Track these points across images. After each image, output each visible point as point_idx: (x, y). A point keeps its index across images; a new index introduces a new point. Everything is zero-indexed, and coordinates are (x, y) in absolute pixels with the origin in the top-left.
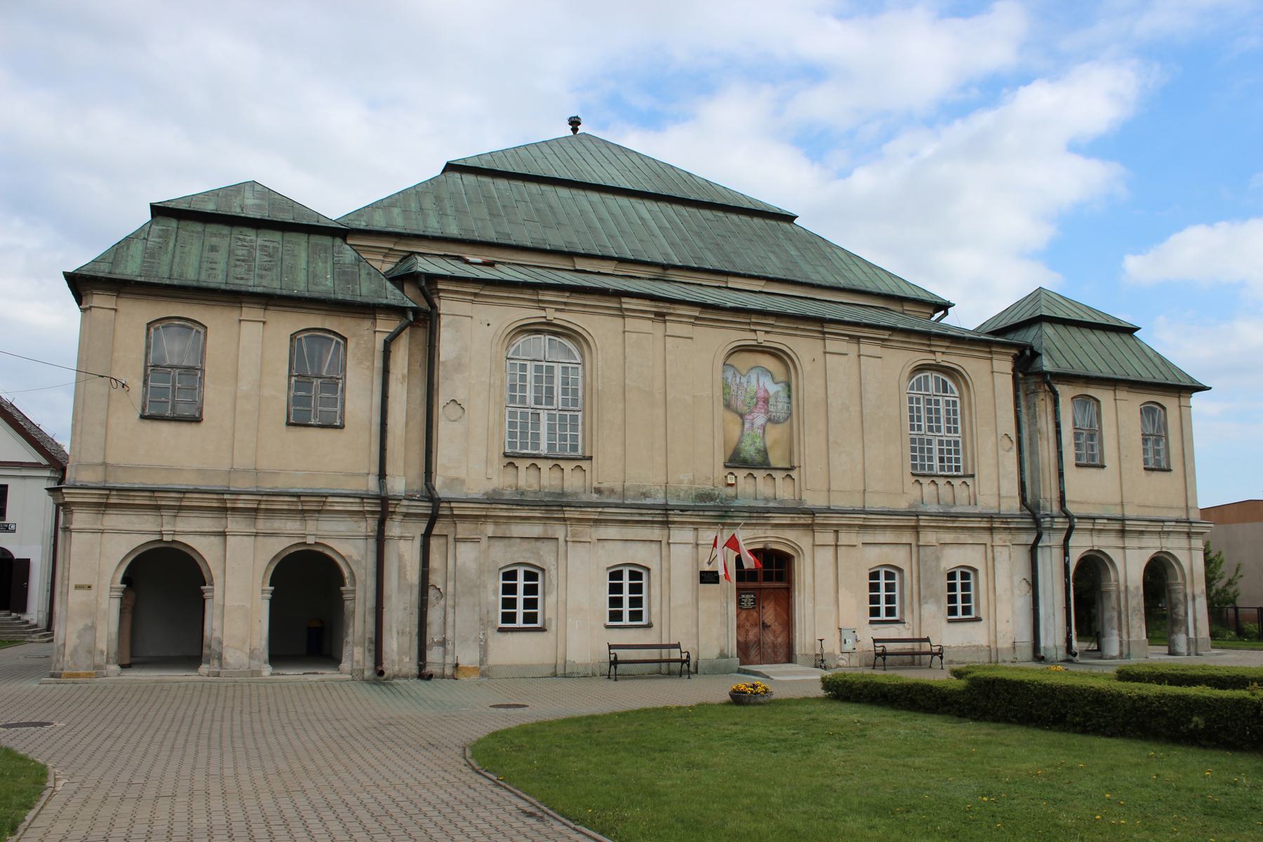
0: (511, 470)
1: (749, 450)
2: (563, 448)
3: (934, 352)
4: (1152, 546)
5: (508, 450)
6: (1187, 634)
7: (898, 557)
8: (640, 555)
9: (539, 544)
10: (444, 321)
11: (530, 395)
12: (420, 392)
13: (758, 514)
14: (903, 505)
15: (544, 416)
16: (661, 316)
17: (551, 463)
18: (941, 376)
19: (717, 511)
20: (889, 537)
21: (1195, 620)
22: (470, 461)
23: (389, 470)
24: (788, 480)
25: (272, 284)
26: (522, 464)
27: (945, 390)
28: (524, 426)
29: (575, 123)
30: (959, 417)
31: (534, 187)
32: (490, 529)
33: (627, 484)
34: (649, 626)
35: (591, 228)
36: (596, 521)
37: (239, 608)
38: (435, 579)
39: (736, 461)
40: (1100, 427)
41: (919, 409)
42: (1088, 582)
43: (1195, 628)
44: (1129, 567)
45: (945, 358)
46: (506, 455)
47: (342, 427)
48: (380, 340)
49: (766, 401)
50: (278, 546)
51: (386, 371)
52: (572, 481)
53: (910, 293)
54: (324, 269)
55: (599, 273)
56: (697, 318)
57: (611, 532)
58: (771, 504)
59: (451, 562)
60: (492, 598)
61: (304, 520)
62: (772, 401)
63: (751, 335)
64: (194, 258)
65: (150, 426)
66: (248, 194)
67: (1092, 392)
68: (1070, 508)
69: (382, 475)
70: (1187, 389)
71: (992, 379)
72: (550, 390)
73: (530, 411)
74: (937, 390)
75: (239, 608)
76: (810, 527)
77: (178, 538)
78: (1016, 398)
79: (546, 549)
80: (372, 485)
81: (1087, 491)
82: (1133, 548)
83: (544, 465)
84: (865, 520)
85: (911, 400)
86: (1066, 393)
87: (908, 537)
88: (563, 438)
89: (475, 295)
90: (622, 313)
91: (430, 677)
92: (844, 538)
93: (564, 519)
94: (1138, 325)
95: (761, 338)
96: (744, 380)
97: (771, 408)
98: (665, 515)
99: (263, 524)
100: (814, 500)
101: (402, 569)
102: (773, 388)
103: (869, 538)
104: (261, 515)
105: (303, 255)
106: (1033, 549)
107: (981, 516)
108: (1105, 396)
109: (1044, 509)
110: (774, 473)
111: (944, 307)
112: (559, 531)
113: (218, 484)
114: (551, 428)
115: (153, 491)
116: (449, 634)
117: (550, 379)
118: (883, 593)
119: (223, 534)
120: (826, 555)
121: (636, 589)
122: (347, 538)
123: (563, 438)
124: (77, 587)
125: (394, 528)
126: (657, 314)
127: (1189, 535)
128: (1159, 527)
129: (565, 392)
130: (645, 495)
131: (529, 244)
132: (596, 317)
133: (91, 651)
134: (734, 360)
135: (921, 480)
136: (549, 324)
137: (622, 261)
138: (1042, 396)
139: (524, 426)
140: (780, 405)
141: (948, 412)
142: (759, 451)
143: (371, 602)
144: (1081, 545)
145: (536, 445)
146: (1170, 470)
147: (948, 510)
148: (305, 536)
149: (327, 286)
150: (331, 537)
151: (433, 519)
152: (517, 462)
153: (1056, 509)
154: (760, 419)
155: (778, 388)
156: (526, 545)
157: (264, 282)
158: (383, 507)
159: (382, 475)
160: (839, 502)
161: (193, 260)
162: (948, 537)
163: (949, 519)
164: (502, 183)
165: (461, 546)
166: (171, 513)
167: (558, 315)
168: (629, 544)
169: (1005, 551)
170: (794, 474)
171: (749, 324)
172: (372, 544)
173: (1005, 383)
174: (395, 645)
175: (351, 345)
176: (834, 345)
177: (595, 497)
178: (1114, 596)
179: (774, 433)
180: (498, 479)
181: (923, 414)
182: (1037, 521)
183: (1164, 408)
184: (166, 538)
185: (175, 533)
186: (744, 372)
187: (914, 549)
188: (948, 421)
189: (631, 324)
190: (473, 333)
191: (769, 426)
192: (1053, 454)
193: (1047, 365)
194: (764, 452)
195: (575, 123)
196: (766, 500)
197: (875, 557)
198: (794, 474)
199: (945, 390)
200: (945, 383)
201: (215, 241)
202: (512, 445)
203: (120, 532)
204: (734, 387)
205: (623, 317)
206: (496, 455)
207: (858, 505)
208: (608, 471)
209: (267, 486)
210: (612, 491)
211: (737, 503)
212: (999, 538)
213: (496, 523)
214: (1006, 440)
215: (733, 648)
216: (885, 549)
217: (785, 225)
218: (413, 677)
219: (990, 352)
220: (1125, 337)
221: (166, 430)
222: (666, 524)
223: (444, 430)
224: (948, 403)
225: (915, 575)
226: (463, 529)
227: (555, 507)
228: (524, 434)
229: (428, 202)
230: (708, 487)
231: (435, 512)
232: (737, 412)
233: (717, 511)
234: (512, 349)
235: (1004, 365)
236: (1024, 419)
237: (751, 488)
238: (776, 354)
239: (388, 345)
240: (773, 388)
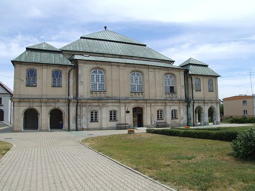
8: (115, 108)
11: (95, 80)
12: (75, 79)
14: (163, 98)
15: (98, 84)
16: (118, 66)
22: (84, 91)
25: (48, 62)
26: (94, 93)
28: (94, 86)
29: (105, 28)
31: (97, 41)
35: (108, 49)
37: (44, 119)
42: (199, 111)
48: (68, 71)
50: (51, 108)
52: (103, 95)
54: (57, 58)
57: (110, 104)
64: (36, 57)
65: (27, 87)
66: (44, 45)
67: (199, 77)
69: (69, 95)
70: (217, 77)
71: (180, 76)
75: (44, 119)
76: (146, 103)
80: (67, 97)
83: (98, 93)
84: (156, 101)
98: (119, 101)
100: (147, 98)
107: (178, 100)
108: (201, 78)
111: (174, 62)
113: (40, 97)
120: (149, 108)
125: (71, 104)
127: (217, 103)
128: (211, 101)
130: (116, 98)
139: (94, 86)
144: (196, 105)
149: (58, 62)
151: (78, 102)
158: (69, 101)
159: (69, 95)
160: (151, 98)
162: (171, 104)
163: (172, 100)
164: (91, 40)
165: (83, 108)
173: (182, 76)
176: (150, 70)
180: (89, 96)
190: (85, 71)
193: (190, 73)
195: (105, 28)
197: (158, 108)
206: (89, 91)
208: (109, 94)
209: (49, 97)
221: (30, 88)
222: (120, 103)
223: (80, 87)
227: (100, 99)
231: (78, 101)
235: (182, 73)
238: (140, 72)
239: (69, 72)
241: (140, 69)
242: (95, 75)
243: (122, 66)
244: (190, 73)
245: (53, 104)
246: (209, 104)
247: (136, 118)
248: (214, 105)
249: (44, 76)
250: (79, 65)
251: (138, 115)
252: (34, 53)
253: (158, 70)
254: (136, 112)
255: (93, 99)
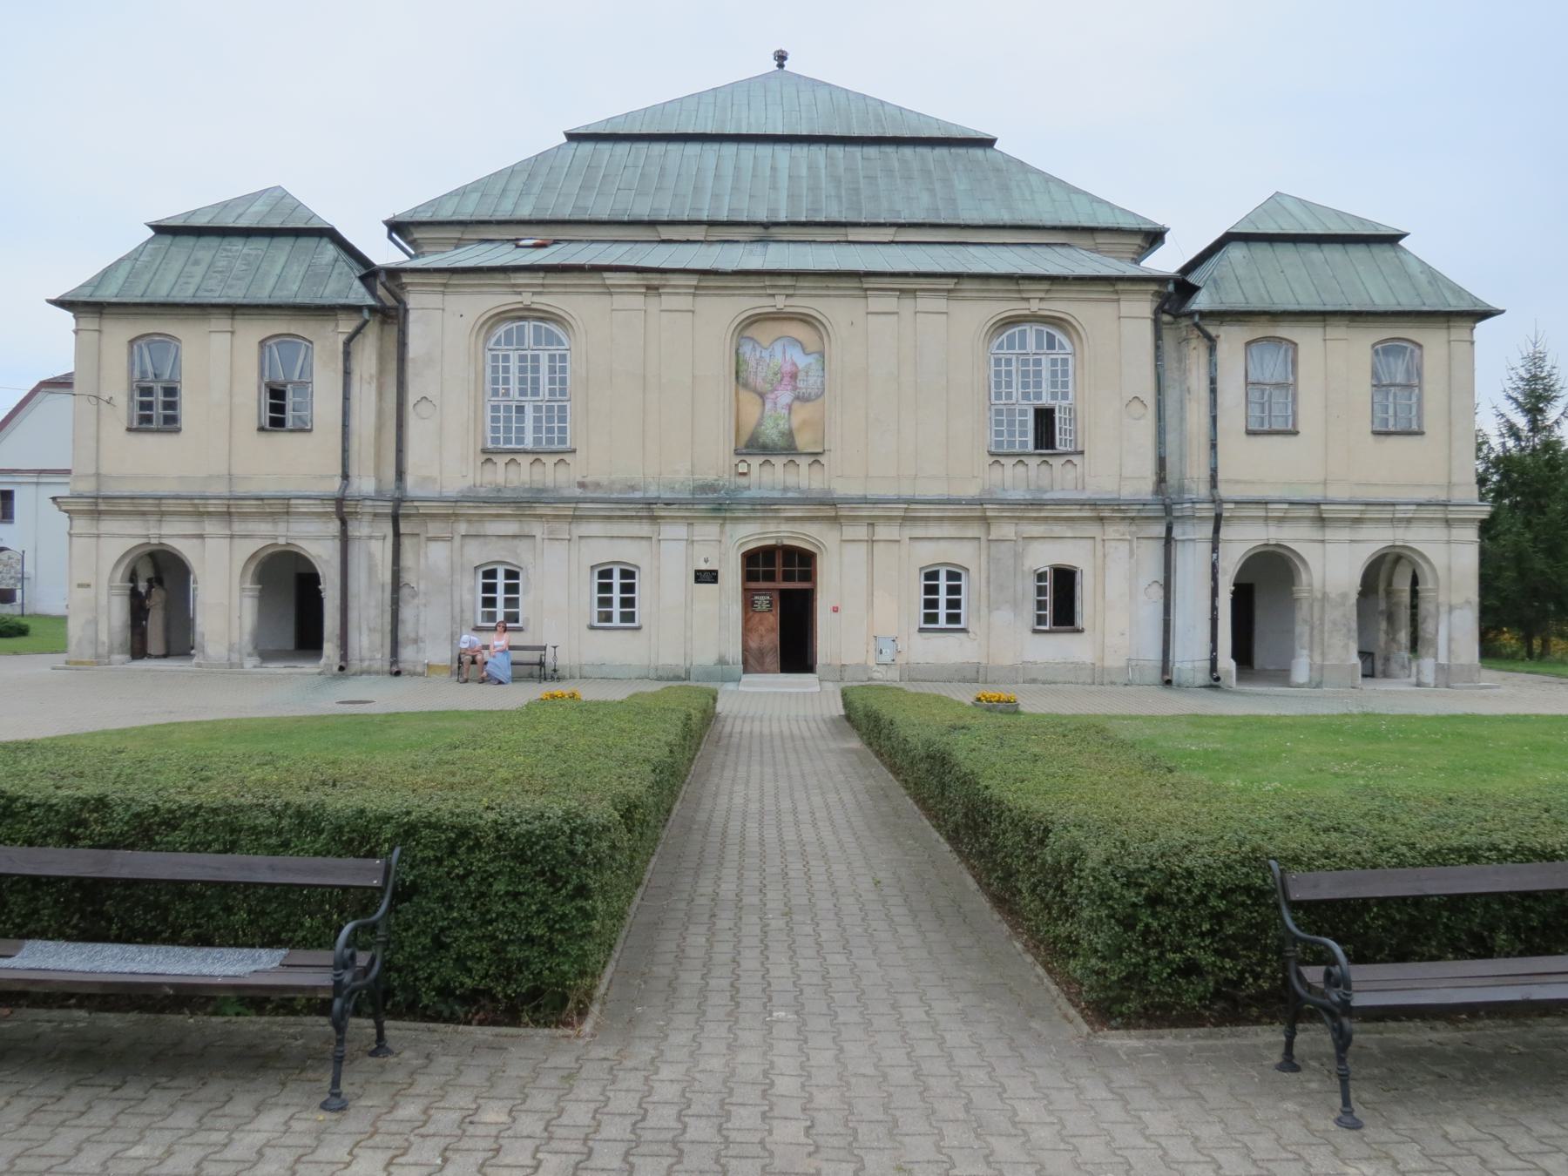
0: (489, 466)
1: (771, 433)
2: (550, 441)
3: (1028, 299)
4: (1377, 539)
5: (490, 445)
6: (1436, 657)
7: (960, 554)
9: (516, 542)
10: (412, 316)
11: (514, 386)
13: (765, 507)
14: (972, 490)
15: (529, 410)
17: (531, 458)
18: (1045, 329)
19: (717, 505)
20: (948, 530)
21: (1450, 640)
22: (443, 459)
23: (354, 471)
24: (816, 466)
26: (501, 460)
27: (1051, 345)
28: (508, 419)
29: (781, 57)
30: (1070, 379)
32: (463, 528)
33: (613, 477)
34: (639, 628)
36: (575, 517)
38: (408, 577)
39: (754, 446)
40: (1296, 380)
41: (1009, 373)
43: (1450, 651)
44: (1333, 568)
45: (1044, 305)
46: (484, 451)
47: (310, 431)
48: (342, 338)
49: (794, 376)
50: (253, 546)
51: (347, 373)
52: (550, 475)
53: (1104, 220)
54: (297, 271)
55: (688, 241)
56: (696, 288)
58: (790, 495)
59: (422, 561)
60: (467, 597)
61: (275, 522)
62: (801, 376)
63: (770, 301)
67: (1284, 331)
68: (1224, 491)
69: (345, 476)
72: (536, 381)
73: (514, 404)
74: (1039, 346)
76: (835, 520)
77: (164, 541)
78: (1157, 348)
79: (522, 545)
81: (1252, 466)
82: (1338, 541)
83: (525, 461)
84: (912, 512)
85: (998, 362)
86: (1231, 340)
87: (974, 530)
88: (550, 430)
89: (445, 285)
90: (608, 291)
91: (398, 673)
92: (883, 532)
93: (541, 516)
94: (1404, 229)
95: (780, 303)
96: (766, 354)
97: (800, 384)
98: (649, 510)
99: (238, 527)
100: (841, 489)
101: (371, 569)
102: (802, 361)
103: (919, 531)
104: (235, 518)
105: (283, 260)
106: (1168, 540)
107: (1082, 504)
108: (1308, 339)
109: (1190, 491)
110: (798, 460)
112: (537, 529)
113: (195, 489)
114: (537, 420)
115: (133, 498)
116: (421, 633)
117: (536, 370)
118: (942, 599)
119: (201, 536)
121: (628, 588)
122: (317, 538)
123: (550, 430)
124: (80, 586)
125: (359, 529)
126: (648, 287)
129: (552, 381)
130: (633, 488)
131: (605, 217)
132: (581, 297)
133: (96, 641)
134: (752, 332)
135: (1003, 460)
136: (528, 309)
137: (712, 224)
138: (1194, 343)
139: (508, 419)
140: (812, 380)
141: (1054, 374)
142: (783, 434)
143: (338, 602)
144: (1241, 542)
145: (520, 440)
146: (1421, 433)
147: (1038, 496)
148: (276, 537)
149: (292, 292)
150: (301, 538)
151: (396, 519)
152: (495, 458)
153: (1203, 491)
154: (785, 397)
155: (811, 359)
156: (502, 543)
157: (231, 293)
159: (345, 476)
161: (171, 277)
165: (433, 546)
166: (155, 518)
167: (536, 299)
168: (616, 541)
169: (1124, 547)
170: (823, 459)
171: (764, 287)
172: (337, 543)
174: (365, 641)
175: (317, 347)
177: (578, 492)
178: (1305, 606)
179: (803, 413)
181: (1016, 380)
182: (1168, 509)
183: (1420, 346)
184: (154, 541)
185: (160, 536)
186: (766, 344)
187: (984, 544)
188: (1054, 384)
189: (620, 301)
190: (442, 326)
191: (797, 404)
192: (1206, 421)
194: (790, 435)
195: (781, 57)
196: (786, 489)
198: (823, 459)
199: (1051, 345)
200: (1051, 338)
201: (200, 254)
202: (495, 440)
203: (113, 536)
204: (752, 363)
205: (611, 294)
207: (907, 492)
209: (240, 490)
210: (598, 485)
211: (747, 494)
212: (1112, 531)
213: (469, 521)
214: (1136, 404)
215: (735, 652)
216: (943, 544)
217: (978, 153)
218: (383, 673)
219: (1116, 292)
220: (1382, 253)
222: (654, 519)
224: (1054, 362)
225: (984, 575)
226: (434, 528)
227: (525, 504)
228: (508, 430)
229: (517, 184)
230: (710, 477)
231: (398, 513)
232: (755, 391)
233: (717, 505)
234: (494, 340)
235: (1141, 308)
236: (1171, 375)
237: (769, 477)
238: (805, 319)
240: (802, 361)
241: (801, 304)
242: (514, 356)
243: (676, 291)
244: (1201, 302)
245: (264, 528)
246: (1365, 532)
247: (773, 620)
248: (1425, 540)
249: (218, 369)
250: (414, 300)
251: (785, 595)
252: (206, 249)
253: (940, 304)
254: (770, 577)
255: (486, 501)
